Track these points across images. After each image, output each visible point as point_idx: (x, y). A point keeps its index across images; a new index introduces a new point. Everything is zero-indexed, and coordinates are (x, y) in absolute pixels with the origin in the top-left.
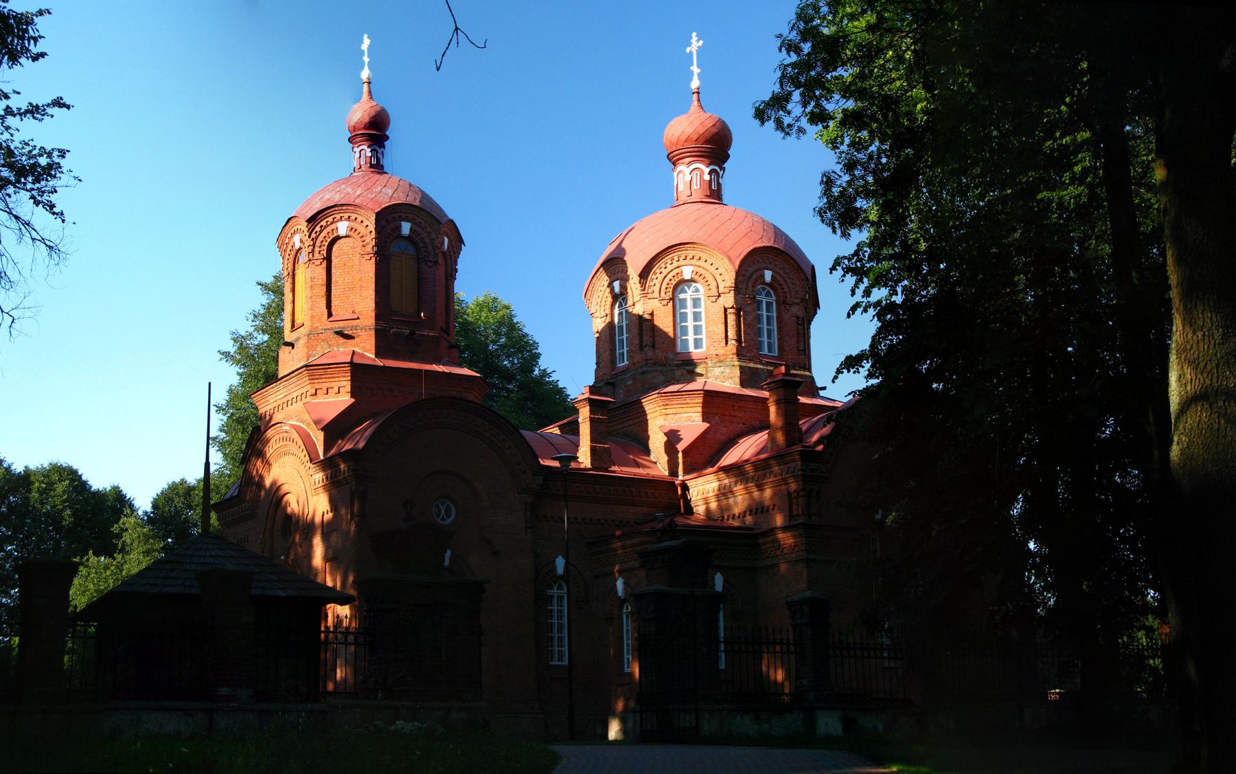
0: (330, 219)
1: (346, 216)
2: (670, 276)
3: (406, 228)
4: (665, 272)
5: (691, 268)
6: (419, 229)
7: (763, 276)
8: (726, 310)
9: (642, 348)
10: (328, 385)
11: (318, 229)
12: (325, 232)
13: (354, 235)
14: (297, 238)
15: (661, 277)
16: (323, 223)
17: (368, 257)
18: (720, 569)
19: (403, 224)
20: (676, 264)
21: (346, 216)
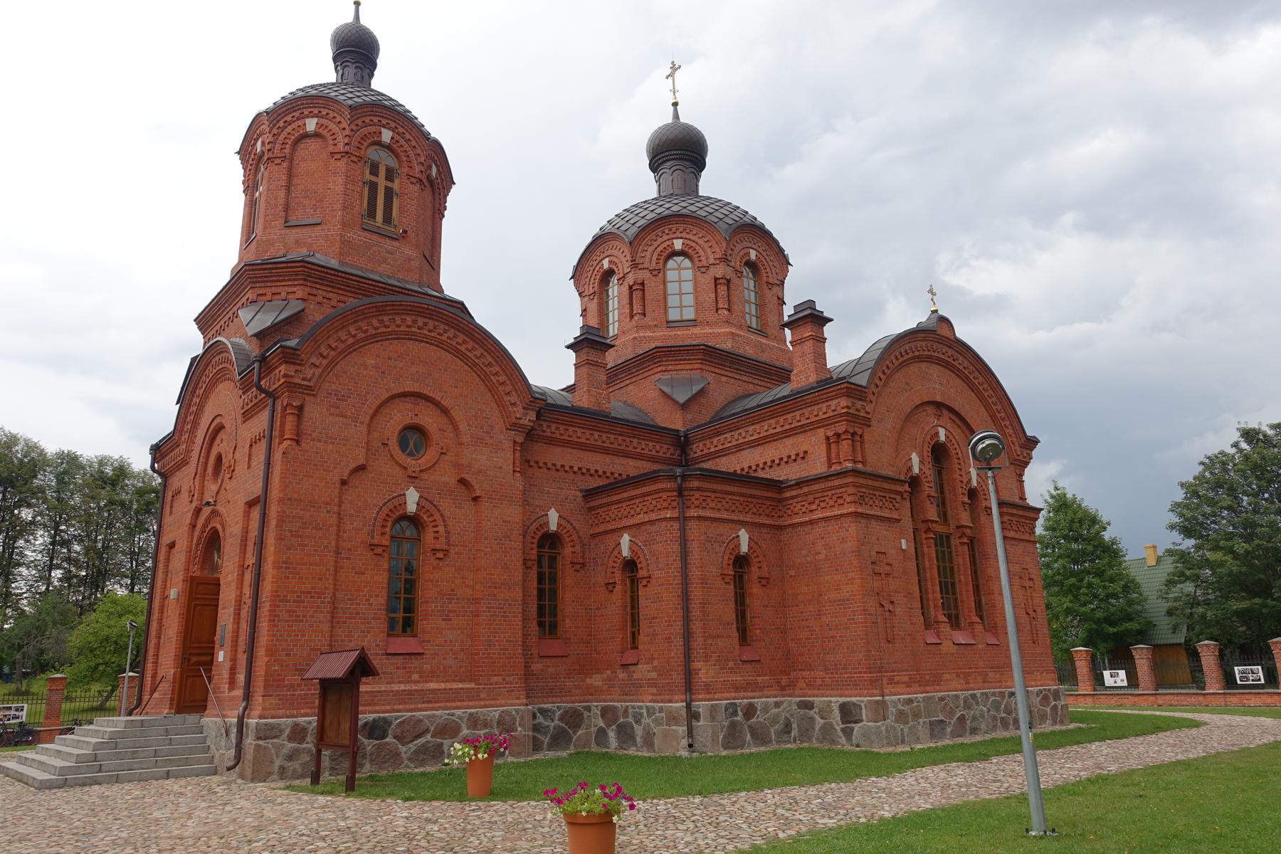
0: (297, 114)
1: (316, 111)
2: (661, 248)
3: (386, 136)
4: (656, 244)
5: (681, 241)
6: (402, 142)
7: (748, 254)
8: (716, 279)
9: (632, 316)
10: (274, 290)
11: (281, 124)
12: (289, 129)
13: (324, 133)
14: (259, 144)
15: (650, 249)
16: (289, 118)
17: (338, 156)
18: (743, 524)
19: (383, 130)
20: (665, 237)
21: (316, 111)
